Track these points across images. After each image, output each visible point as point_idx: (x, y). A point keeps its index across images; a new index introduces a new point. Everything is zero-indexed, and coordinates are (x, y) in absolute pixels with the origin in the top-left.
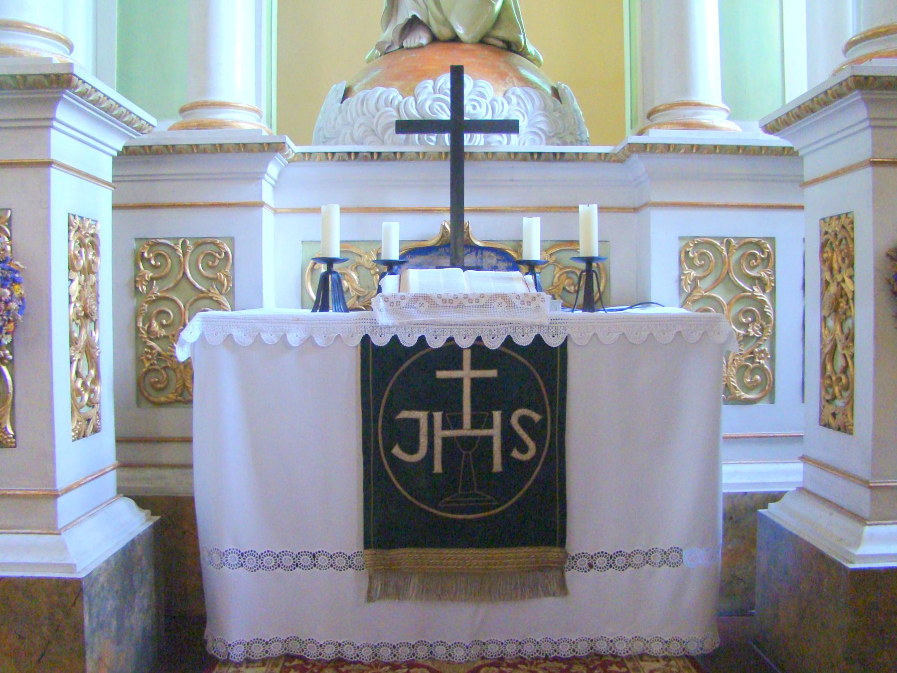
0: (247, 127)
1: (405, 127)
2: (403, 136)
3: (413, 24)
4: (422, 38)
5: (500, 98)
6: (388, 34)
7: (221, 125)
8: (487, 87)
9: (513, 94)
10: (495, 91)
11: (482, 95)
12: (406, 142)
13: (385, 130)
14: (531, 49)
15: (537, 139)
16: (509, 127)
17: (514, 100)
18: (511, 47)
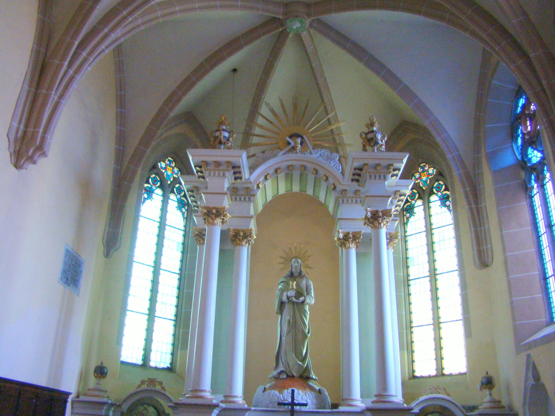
0: (241, 402)
1: (280, 404)
2: (279, 406)
3: (282, 372)
4: (285, 376)
5: (304, 395)
6: (275, 373)
7: (234, 402)
8: (301, 392)
9: (307, 394)
10: (303, 393)
11: (299, 395)
12: (279, 408)
13: (275, 402)
14: (314, 377)
15: (313, 406)
16: (305, 405)
17: (307, 395)
18: (308, 378)
